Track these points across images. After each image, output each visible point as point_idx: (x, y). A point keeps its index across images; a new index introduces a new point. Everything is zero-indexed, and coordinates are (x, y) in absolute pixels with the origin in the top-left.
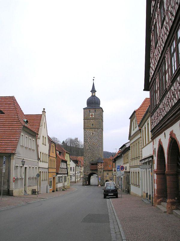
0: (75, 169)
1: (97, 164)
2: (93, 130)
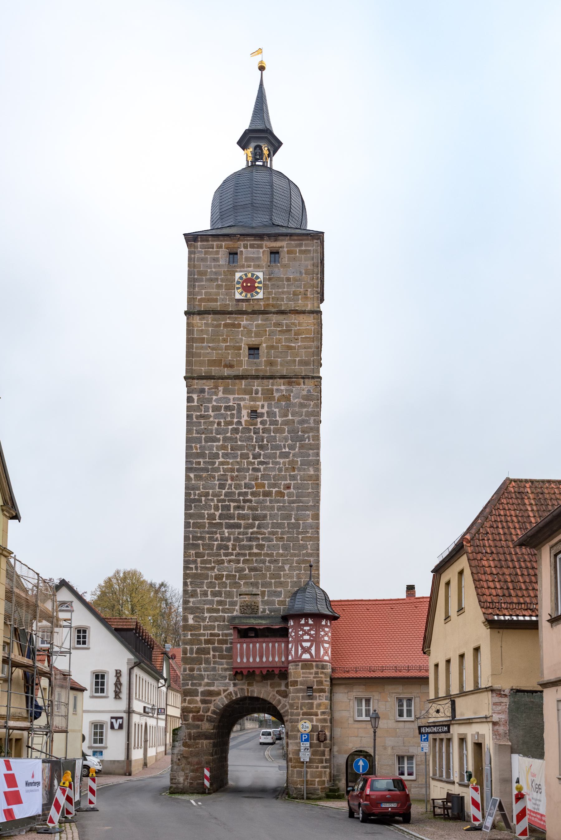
0: (124, 680)
1: (283, 633)
2: (257, 385)
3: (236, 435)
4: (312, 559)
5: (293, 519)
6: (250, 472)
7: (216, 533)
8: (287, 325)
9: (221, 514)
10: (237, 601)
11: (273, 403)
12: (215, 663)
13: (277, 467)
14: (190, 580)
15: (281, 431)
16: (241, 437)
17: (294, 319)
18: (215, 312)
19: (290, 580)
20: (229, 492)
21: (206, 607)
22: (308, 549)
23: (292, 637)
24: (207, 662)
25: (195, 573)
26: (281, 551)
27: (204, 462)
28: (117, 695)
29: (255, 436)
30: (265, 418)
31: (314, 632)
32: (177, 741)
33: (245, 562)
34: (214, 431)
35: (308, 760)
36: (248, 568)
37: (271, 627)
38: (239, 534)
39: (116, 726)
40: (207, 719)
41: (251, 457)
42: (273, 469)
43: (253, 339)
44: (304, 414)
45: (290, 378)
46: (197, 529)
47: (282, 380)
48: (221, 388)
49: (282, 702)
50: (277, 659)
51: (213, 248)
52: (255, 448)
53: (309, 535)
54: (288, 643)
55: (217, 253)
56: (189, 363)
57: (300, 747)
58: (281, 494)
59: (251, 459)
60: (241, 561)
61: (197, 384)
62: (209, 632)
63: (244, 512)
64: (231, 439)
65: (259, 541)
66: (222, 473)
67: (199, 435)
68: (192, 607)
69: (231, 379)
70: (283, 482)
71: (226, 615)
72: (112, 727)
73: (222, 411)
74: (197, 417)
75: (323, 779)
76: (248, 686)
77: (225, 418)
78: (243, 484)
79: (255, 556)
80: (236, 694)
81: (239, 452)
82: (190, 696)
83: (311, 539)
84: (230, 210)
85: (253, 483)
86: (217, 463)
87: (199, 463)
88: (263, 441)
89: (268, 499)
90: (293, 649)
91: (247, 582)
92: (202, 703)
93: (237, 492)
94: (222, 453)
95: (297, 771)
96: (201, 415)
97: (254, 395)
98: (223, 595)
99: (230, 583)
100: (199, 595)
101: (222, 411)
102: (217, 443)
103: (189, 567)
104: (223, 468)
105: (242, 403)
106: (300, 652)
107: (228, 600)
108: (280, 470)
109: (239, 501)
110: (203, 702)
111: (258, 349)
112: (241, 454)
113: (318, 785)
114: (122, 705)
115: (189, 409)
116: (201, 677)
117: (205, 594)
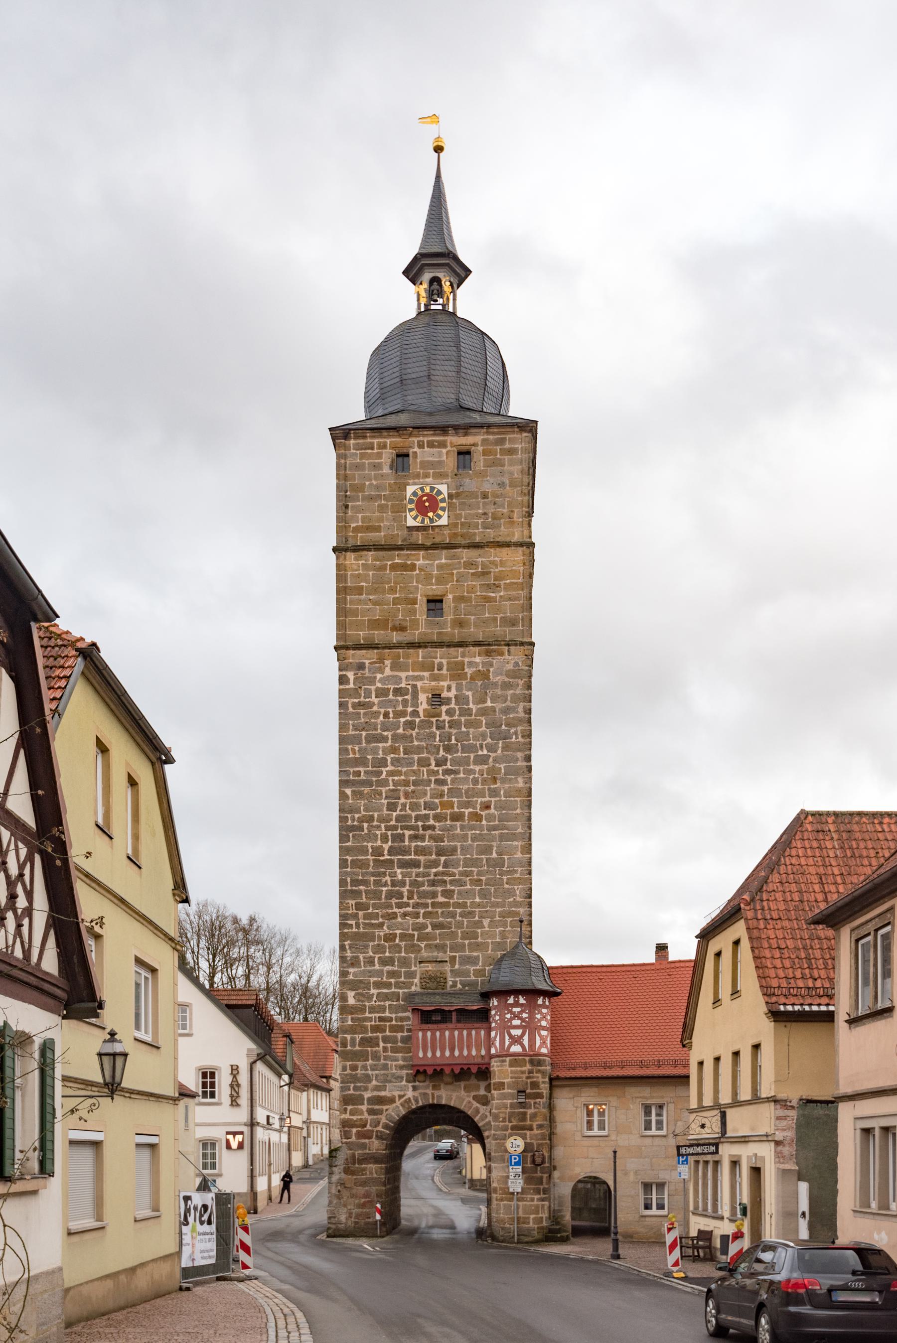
1: (483, 1015)
2: (440, 657)
3: (411, 732)
7: (384, 874)
8: (484, 565)
9: (391, 847)
11: (464, 682)
13: (471, 777)
16: (418, 734)
21: (372, 980)
23: (496, 1022)
24: (376, 1057)
27: (365, 772)
29: (438, 733)
30: (453, 706)
33: (427, 915)
35: (519, 1190)
38: (417, 875)
40: (377, 1136)
41: (433, 763)
42: (466, 780)
43: (434, 587)
44: (509, 698)
45: (489, 645)
47: (477, 649)
48: (388, 663)
49: (482, 1111)
50: (474, 1053)
54: (489, 1029)
56: (341, 625)
59: (433, 767)
62: (378, 1015)
63: (424, 844)
64: (404, 737)
65: (446, 886)
69: (402, 647)
70: (479, 800)
71: (401, 991)
73: (391, 697)
74: (354, 706)
75: (540, 1215)
79: (441, 908)
80: (417, 1101)
81: (416, 757)
82: (353, 1105)
83: (520, 881)
85: (437, 801)
86: (385, 773)
87: (358, 774)
88: (450, 740)
89: (458, 824)
90: (498, 1039)
91: (430, 945)
93: (413, 814)
95: (504, 1205)
97: (436, 671)
99: (405, 946)
101: (391, 697)
102: (385, 745)
104: (393, 780)
105: (419, 684)
106: (507, 1043)
109: (416, 828)
110: (371, 1112)
111: (441, 601)
112: (419, 759)
113: (534, 1223)
116: (368, 1079)
117: (371, 962)
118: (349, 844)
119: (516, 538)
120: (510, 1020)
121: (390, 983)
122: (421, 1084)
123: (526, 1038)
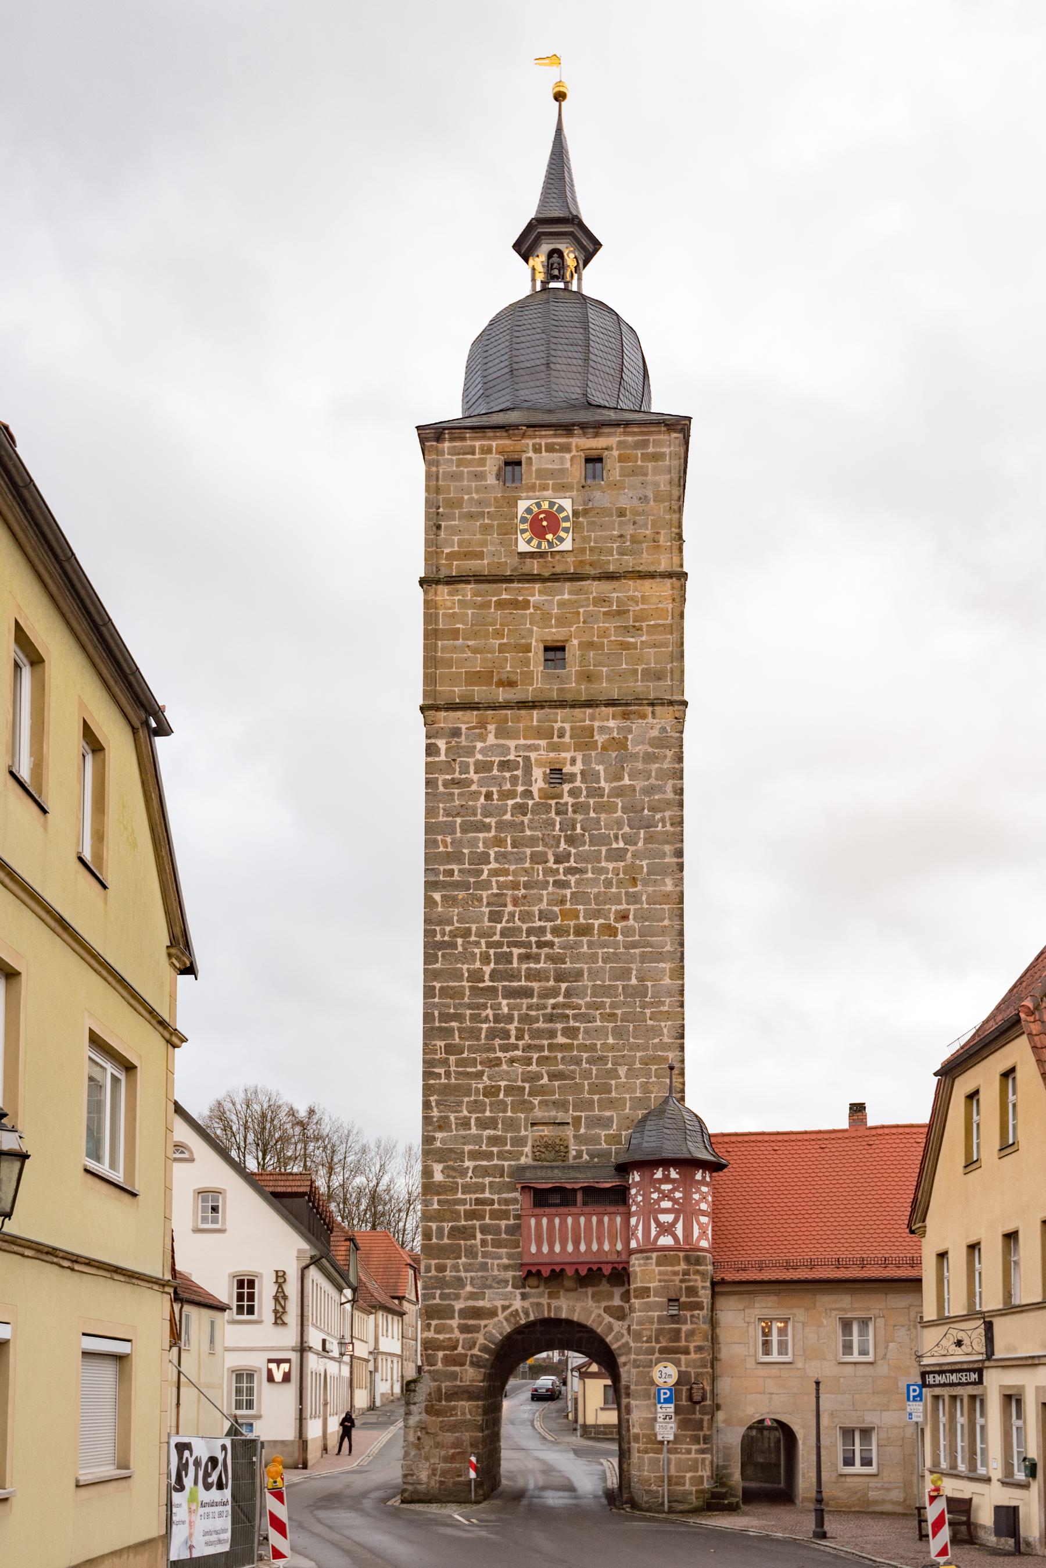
0: (292, 1289)
1: (619, 1196)
2: (561, 720)
3: (522, 818)
4: (671, 1055)
5: (633, 978)
6: (550, 889)
7: (485, 1006)
8: (619, 602)
9: (493, 971)
10: (527, 1136)
11: (593, 753)
12: (485, 1255)
13: (603, 877)
14: (435, 1097)
15: (607, 808)
16: (531, 821)
17: (634, 588)
18: (479, 579)
19: (628, 1096)
20: (509, 928)
21: (467, 1148)
22: (662, 1034)
23: (637, 1204)
24: (471, 1253)
25: (446, 1086)
26: (611, 1041)
27: (460, 871)
28: (279, 1319)
29: (558, 819)
30: (578, 784)
31: (681, 1195)
32: (415, 1404)
33: (541, 1061)
34: (479, 811)
35: (671, 1438)
36: (548, 1073)
37: (596, 1185)
38: (529, 1008)
39: (278, 1376)
41: (552, 859)
43: (554, 630)
44: (653, 774)
45: (627, 704)
46: (449, 1000)
47: (611, 710)
48: (491, 727)
49: (616, 1329)
50: (606, 1247)
51: (473, 453)
52: (559, 842)
53: (666, 1008)
54: (628, 1215)
55: (482, 462)
56: (429, 679)
57: (656, 1412)
58: (611, 931)
60: (534, 1061)
61: (445, 719)
62: (473, 1196)
63: (538, 966)
64: (512, 825)
65: (568, 1022)
66: (495, 891)
67: (450, 819)
68: (440, 1149)
69: (511, 708)
70: (614, 908)
71: (506, 1164)
72: (271, 1379)
73: (495, 772)
74: (446, 784)
75: (700, 1473)
76: (550, 1297)
77: (500, 785)
78: (537, 912)
79: (561, 1051)
80: (527, 1314)
81: (528, 851)
82: (439, 1319)
84: (503, 378)
85: (556, 909)
86: (486, 872)
87: (451, 873)
88: (574, 829)
89: (585, 939)
90: (640, 1228)
91: (546, 1101)
92: (462, 1332)
93: (525, 927)
94: (496, 852)
95: (650, 1459)
96: (453, 779)
97: (556, 739)
98: (500, 1126)
99: (512, 1102)
100: (454, 1126)
101: (495, 772)
102: (486, 835)
103: (433, 1073)
104: (497, 882)
105: (533, 756)
107: (509, 1135)
108: (608, 883)
109: (528, 945)
110: (464, 1329)
111: (563, 649)
112: (532, 854)
113: (691, 1484)
114: (289, 1336)
115: (430, 767)
116: (460, 1282)
117: (465, 1124)
118: (438, 966)
119: (663, 566)
120: (658, 1201)
121: (492, 1152)
122: (533, 1291)
123: (680, 1226)
